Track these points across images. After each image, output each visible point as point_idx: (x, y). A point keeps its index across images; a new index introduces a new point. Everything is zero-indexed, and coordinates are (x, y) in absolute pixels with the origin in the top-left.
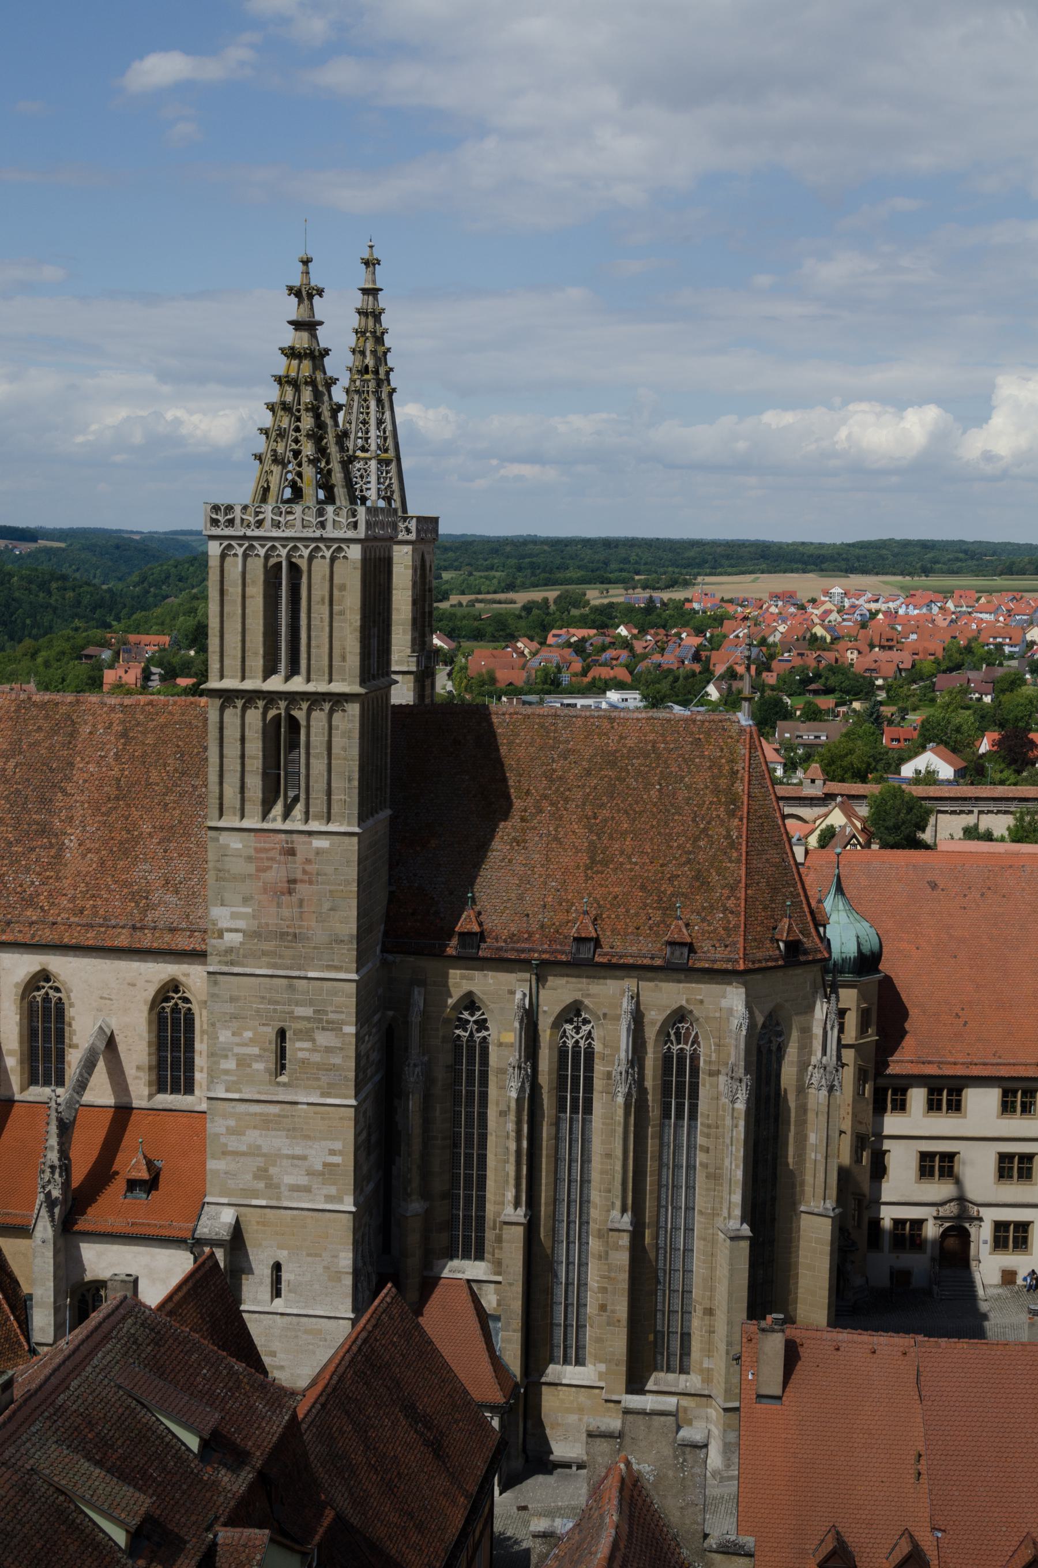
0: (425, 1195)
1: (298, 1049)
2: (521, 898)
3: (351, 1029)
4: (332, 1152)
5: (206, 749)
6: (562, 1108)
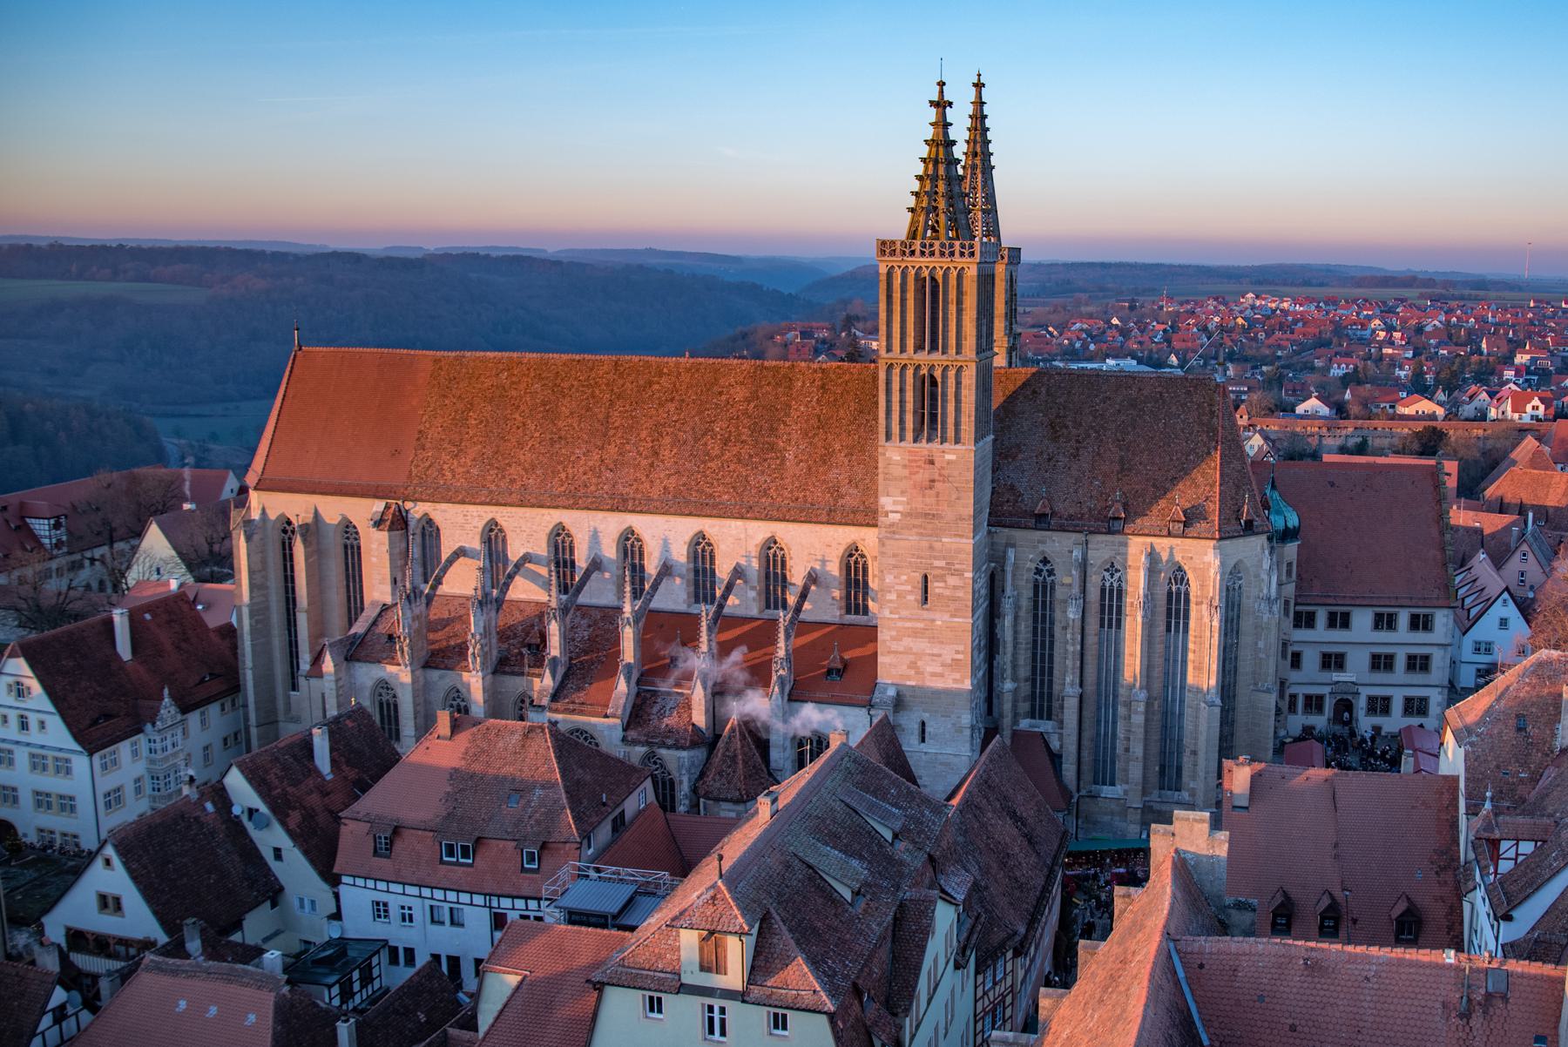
0: (1015, 679)
1: (936, 587)
2: (1076, 492)
3: (970, 575)
4: (958, 652)
5: (876, 396)
6: (1102, 626)
